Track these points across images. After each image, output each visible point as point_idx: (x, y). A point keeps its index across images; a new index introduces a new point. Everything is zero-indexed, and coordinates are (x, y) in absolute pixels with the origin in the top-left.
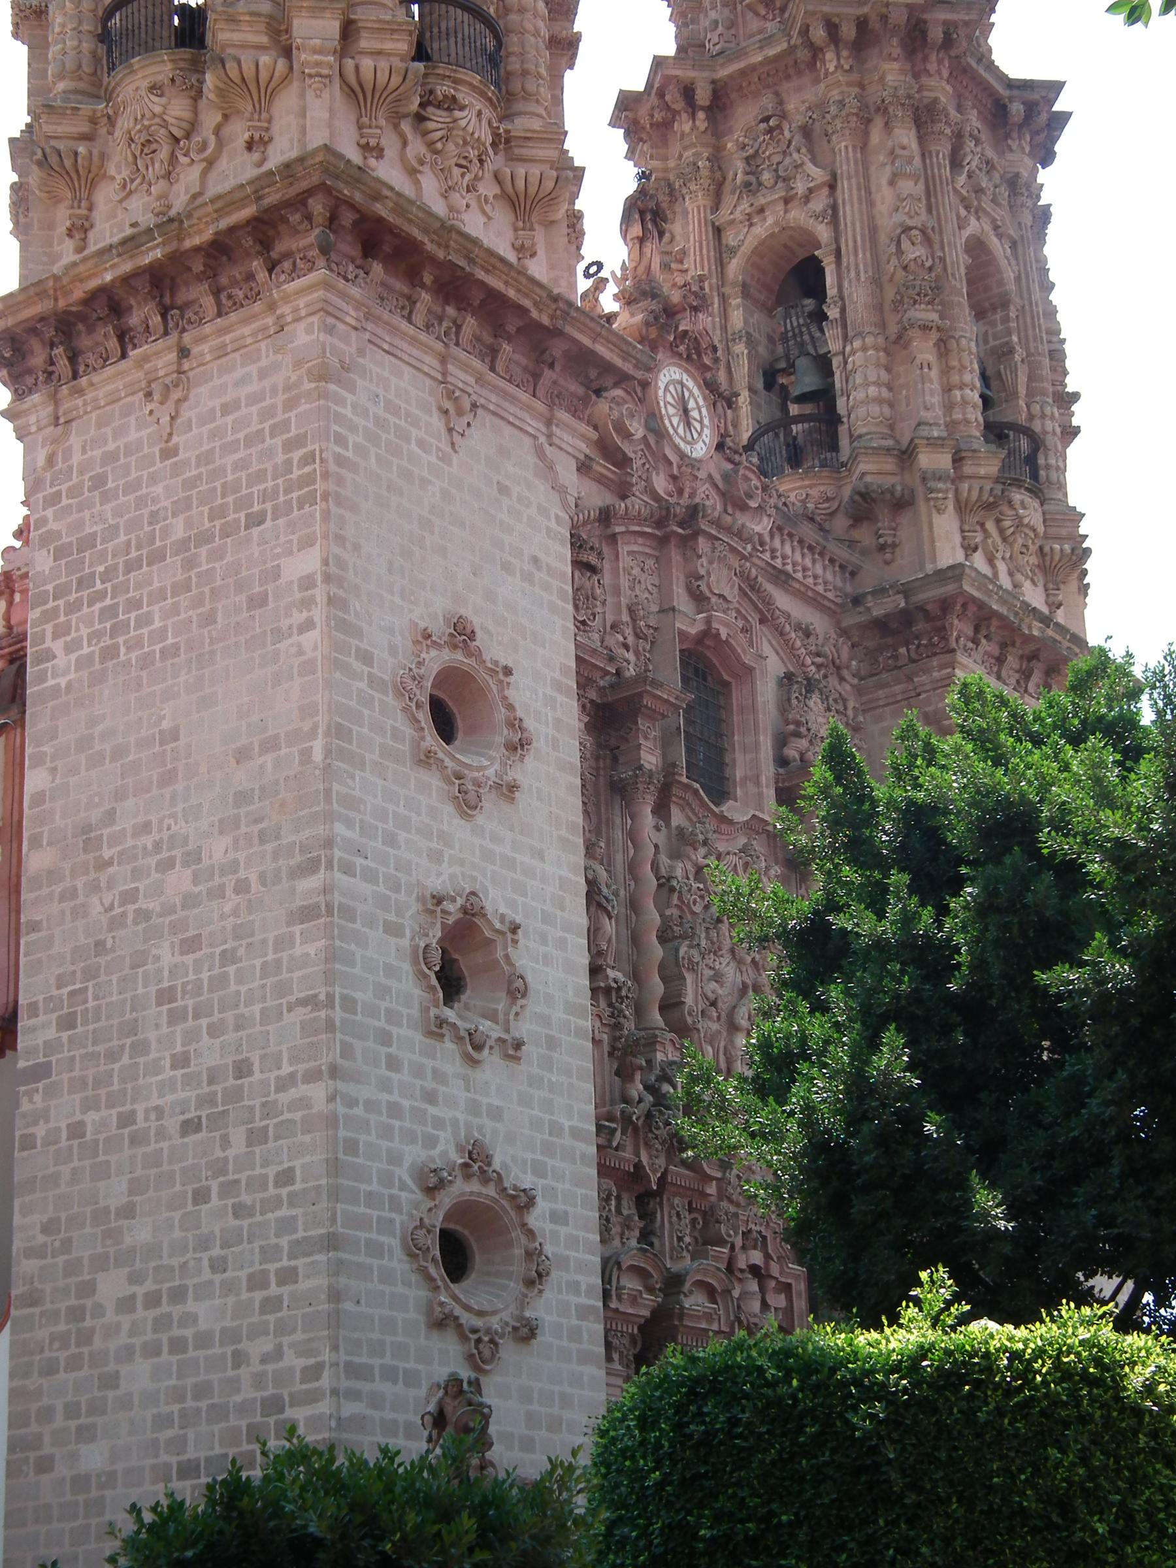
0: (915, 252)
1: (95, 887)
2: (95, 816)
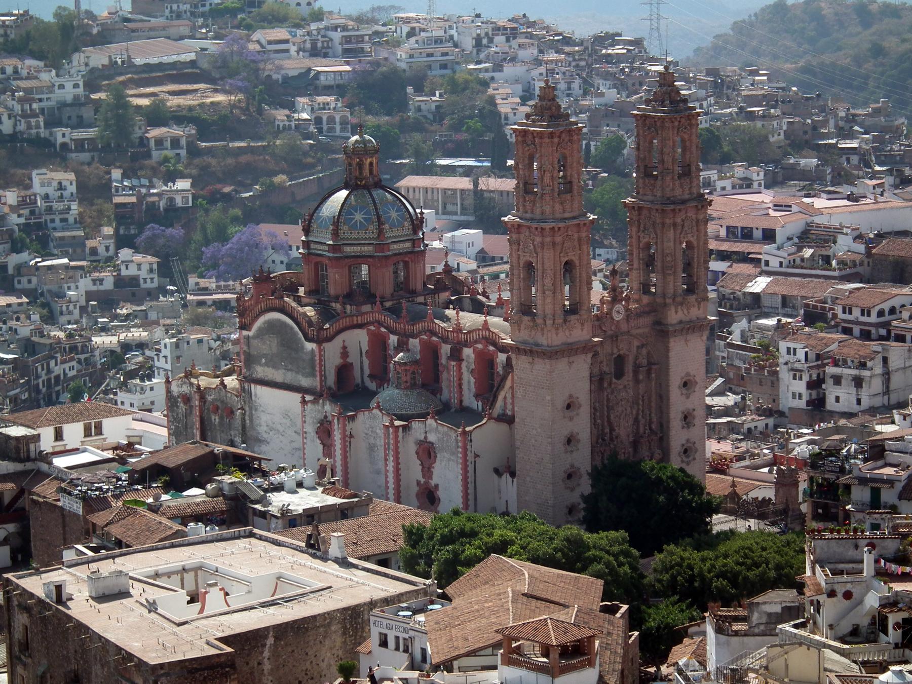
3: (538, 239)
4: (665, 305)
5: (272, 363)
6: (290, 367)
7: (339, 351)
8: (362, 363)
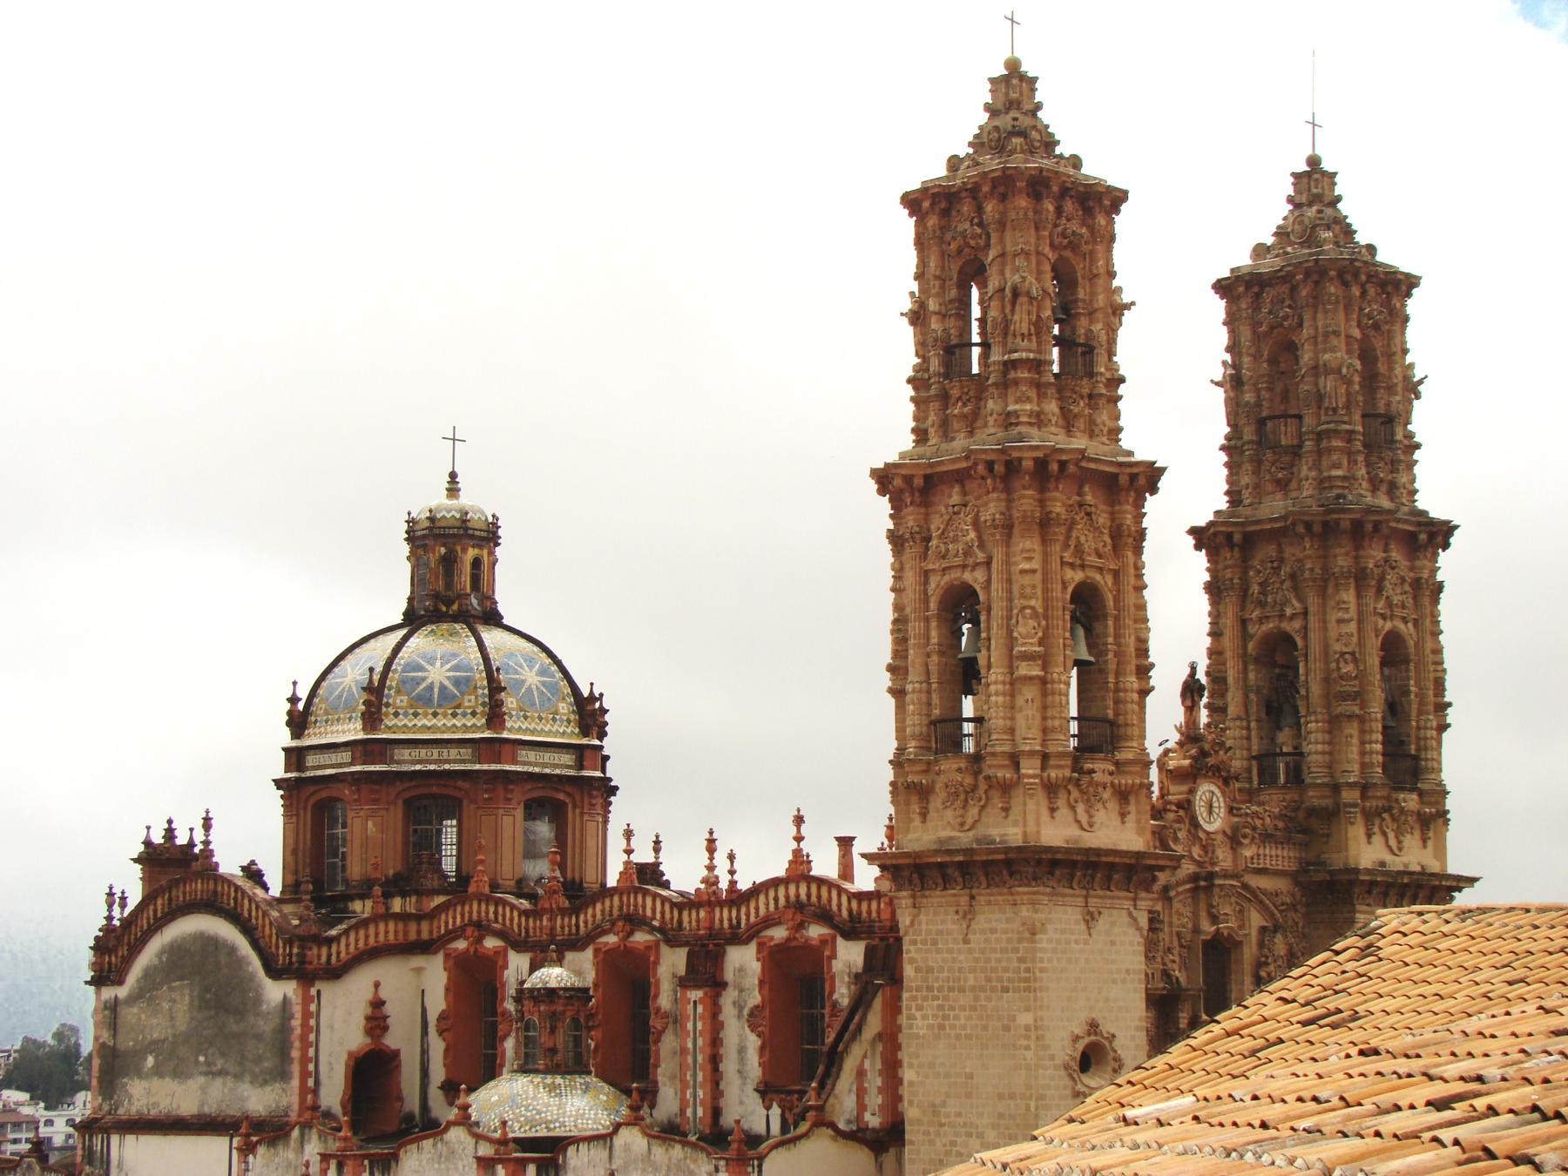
0: (1348, 668)
1: (938, 1134)
2: (938, 1101)
3: (992, 509)
5: (174, 1064)
6: (220, 1063)
7: (360, 1011)
8: (424, 1052)
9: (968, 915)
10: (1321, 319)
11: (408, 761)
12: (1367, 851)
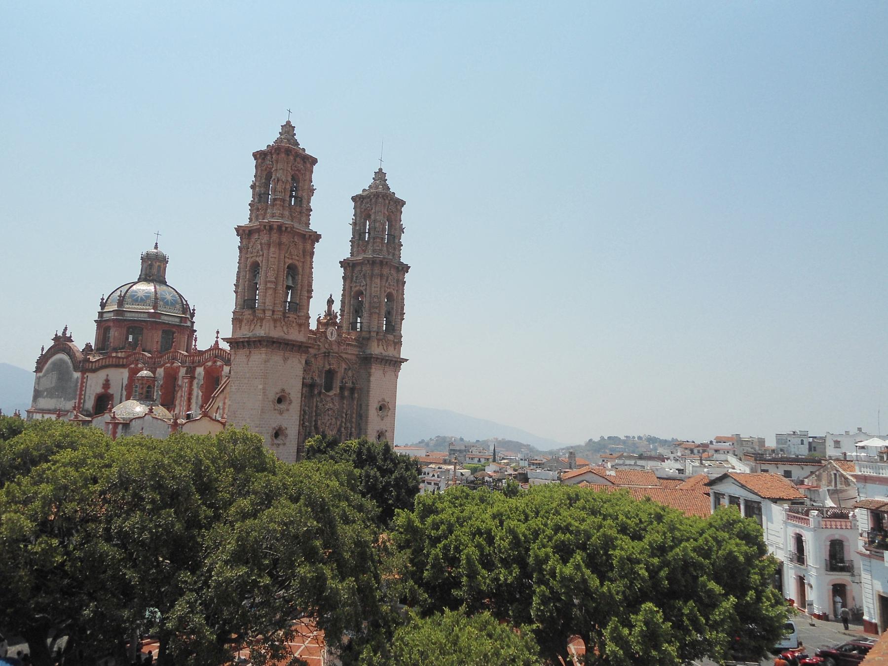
3: (265, 239)
4: (369, 339)
7: (101, 381)
9: (248, 356)
10: (378, 210)
11: (128, 316)
12: (376, 349)
